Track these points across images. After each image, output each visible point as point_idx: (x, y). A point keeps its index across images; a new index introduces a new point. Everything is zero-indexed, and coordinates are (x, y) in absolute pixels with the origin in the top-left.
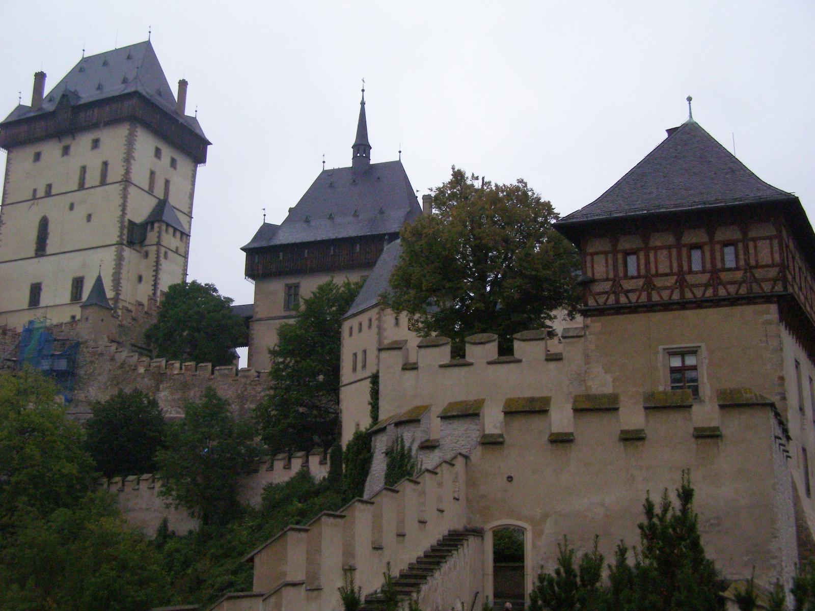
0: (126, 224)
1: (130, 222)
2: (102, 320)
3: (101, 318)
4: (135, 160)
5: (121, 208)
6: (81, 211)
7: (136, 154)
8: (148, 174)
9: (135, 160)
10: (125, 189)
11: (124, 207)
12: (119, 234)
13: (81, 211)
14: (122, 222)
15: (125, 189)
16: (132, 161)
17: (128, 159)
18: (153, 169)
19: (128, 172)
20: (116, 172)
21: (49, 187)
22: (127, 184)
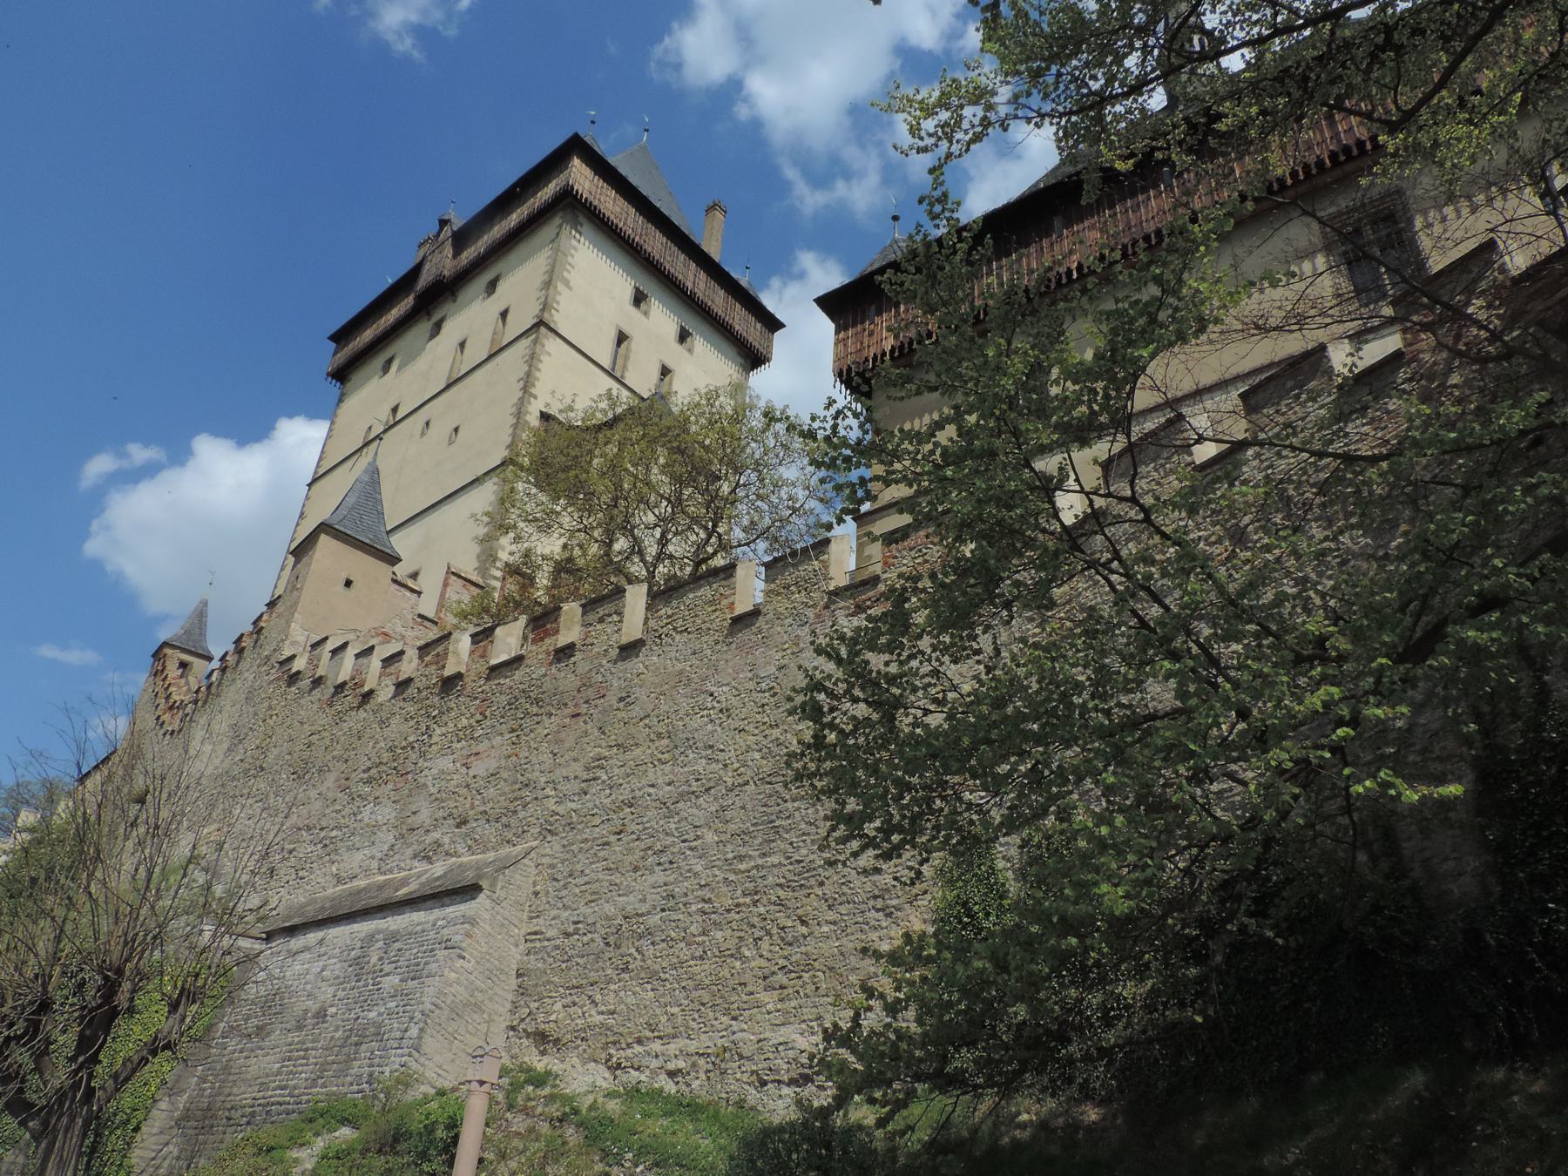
0: (533, 420)
1: (545, 417)
2: (348, 583)
3: (343, 576)
4: (570, 288)
5: (522, 384)
6: (440, 430)
7: (573, 276)
8: (612, 337)
9: (570, 288)
10: (535, 342)
11: (527, 383)
12: (509, 440)
13: (440, 430)
14: (519, 413)
15: (535, 342)
16: (561, 287)
17: (548, 284)
18: (627, 330)
19: (545, 306)
20: (521, 320)
21: (395, 410)
22: (543, 329)
